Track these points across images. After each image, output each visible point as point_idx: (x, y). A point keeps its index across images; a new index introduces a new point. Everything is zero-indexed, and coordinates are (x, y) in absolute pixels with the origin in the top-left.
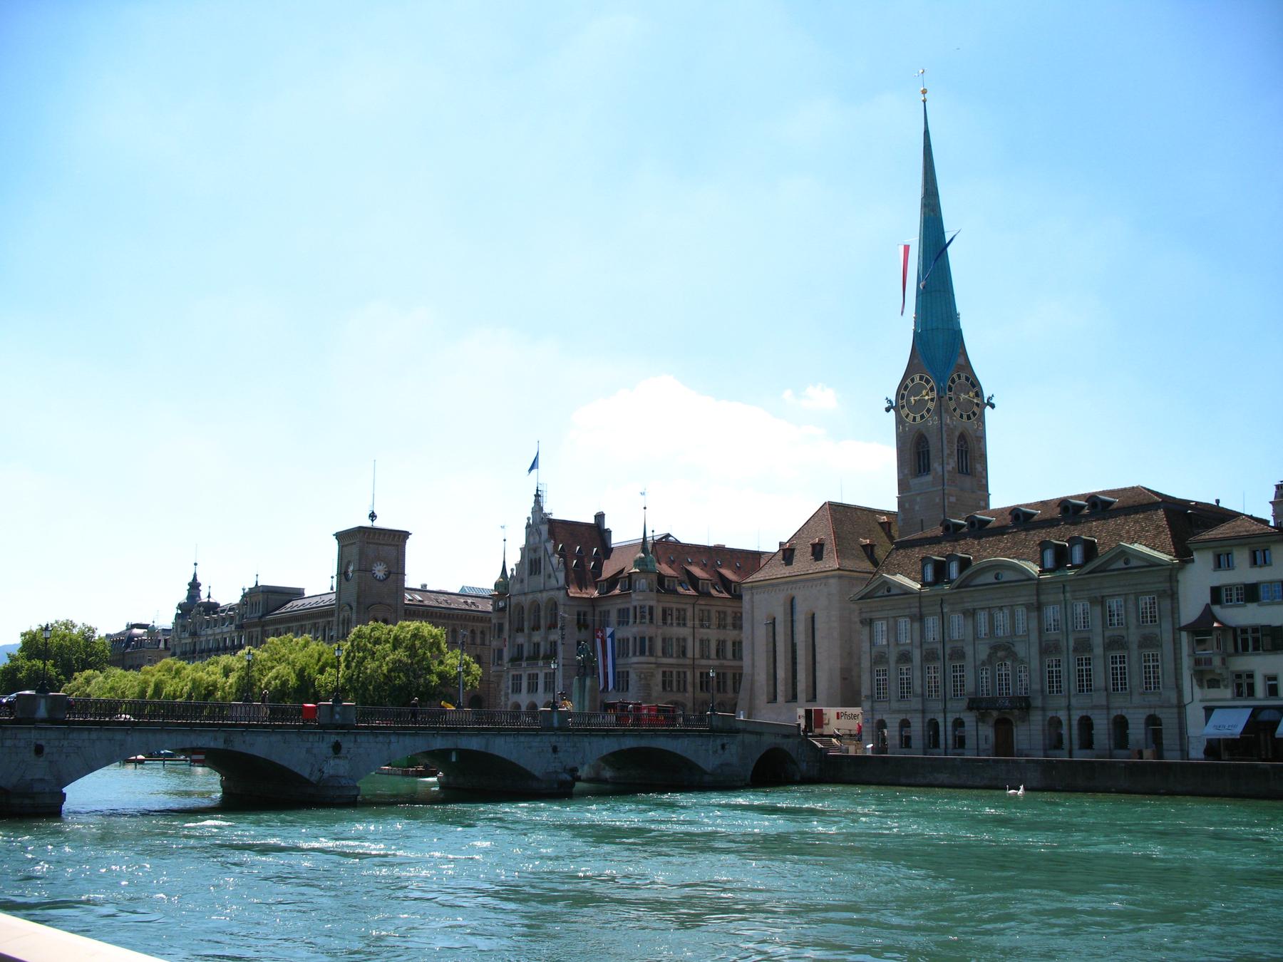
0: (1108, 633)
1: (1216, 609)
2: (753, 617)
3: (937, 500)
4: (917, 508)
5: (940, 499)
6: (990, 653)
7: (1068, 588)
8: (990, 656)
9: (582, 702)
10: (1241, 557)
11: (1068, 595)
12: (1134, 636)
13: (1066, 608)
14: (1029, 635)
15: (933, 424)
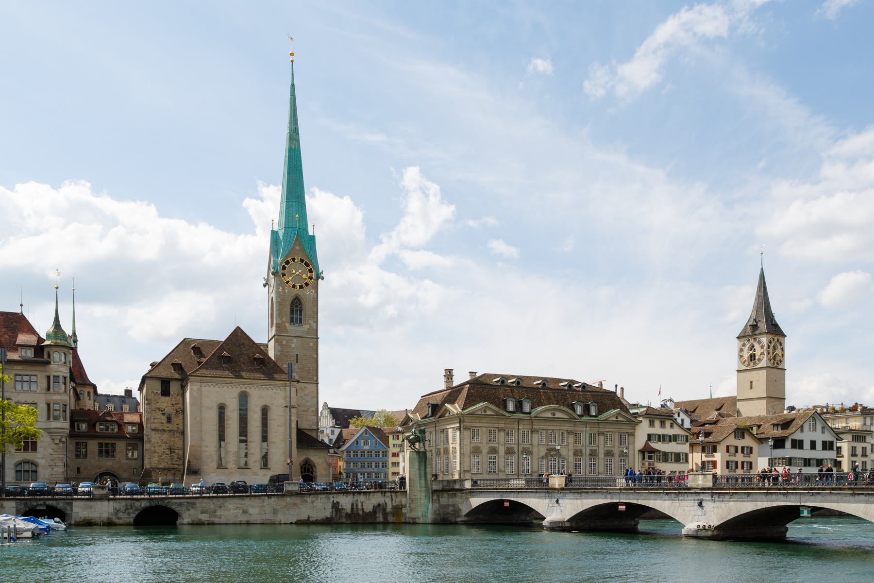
0: (606, 449)
1: (649, 442)
2: (201, 403)
3: (311, 344)
4: (293, 346)
5: (313, 344)
6: (547, 453)
7: (588, 425)
8: (546, 454)
9: (423, 469)
10: (657, 423)
11: (588, 428)
12: (616, 451)
13: (586, 434)
14: (568, 446)
15: (309, 294)
